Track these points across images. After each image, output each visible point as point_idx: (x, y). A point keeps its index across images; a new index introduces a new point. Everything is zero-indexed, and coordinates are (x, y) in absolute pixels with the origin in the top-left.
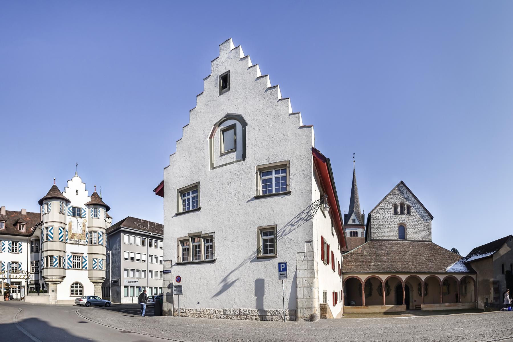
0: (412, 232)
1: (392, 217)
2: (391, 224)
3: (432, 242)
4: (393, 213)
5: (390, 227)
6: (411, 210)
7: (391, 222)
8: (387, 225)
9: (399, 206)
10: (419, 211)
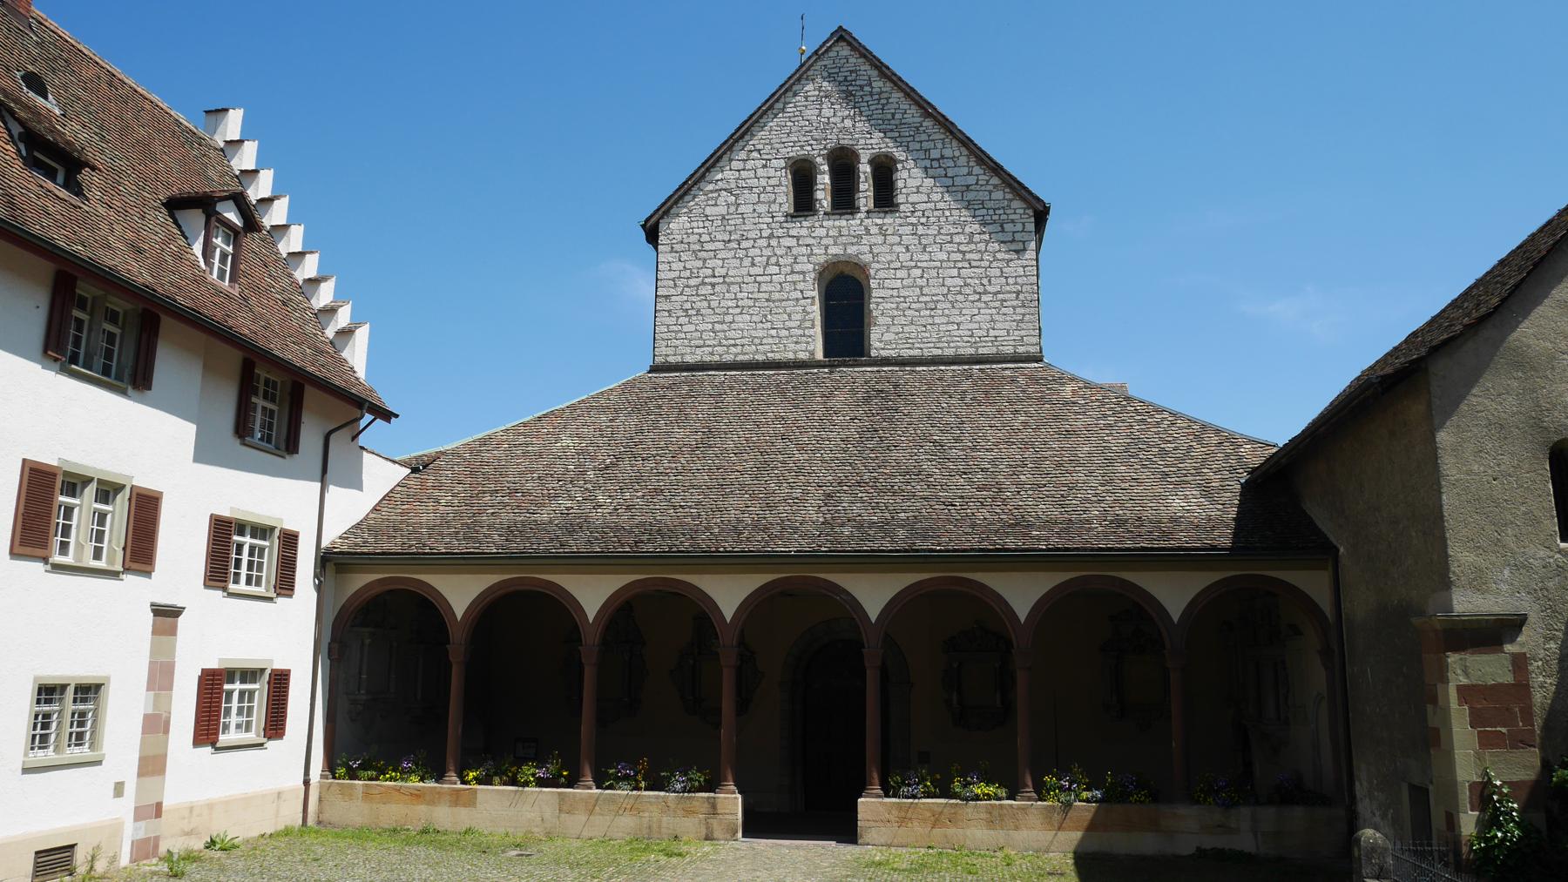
1: (780, 232)
2: (775, 269)
4: (788, 207)
6: (900, 184)
7: (773, 260)
9: (826, 168)
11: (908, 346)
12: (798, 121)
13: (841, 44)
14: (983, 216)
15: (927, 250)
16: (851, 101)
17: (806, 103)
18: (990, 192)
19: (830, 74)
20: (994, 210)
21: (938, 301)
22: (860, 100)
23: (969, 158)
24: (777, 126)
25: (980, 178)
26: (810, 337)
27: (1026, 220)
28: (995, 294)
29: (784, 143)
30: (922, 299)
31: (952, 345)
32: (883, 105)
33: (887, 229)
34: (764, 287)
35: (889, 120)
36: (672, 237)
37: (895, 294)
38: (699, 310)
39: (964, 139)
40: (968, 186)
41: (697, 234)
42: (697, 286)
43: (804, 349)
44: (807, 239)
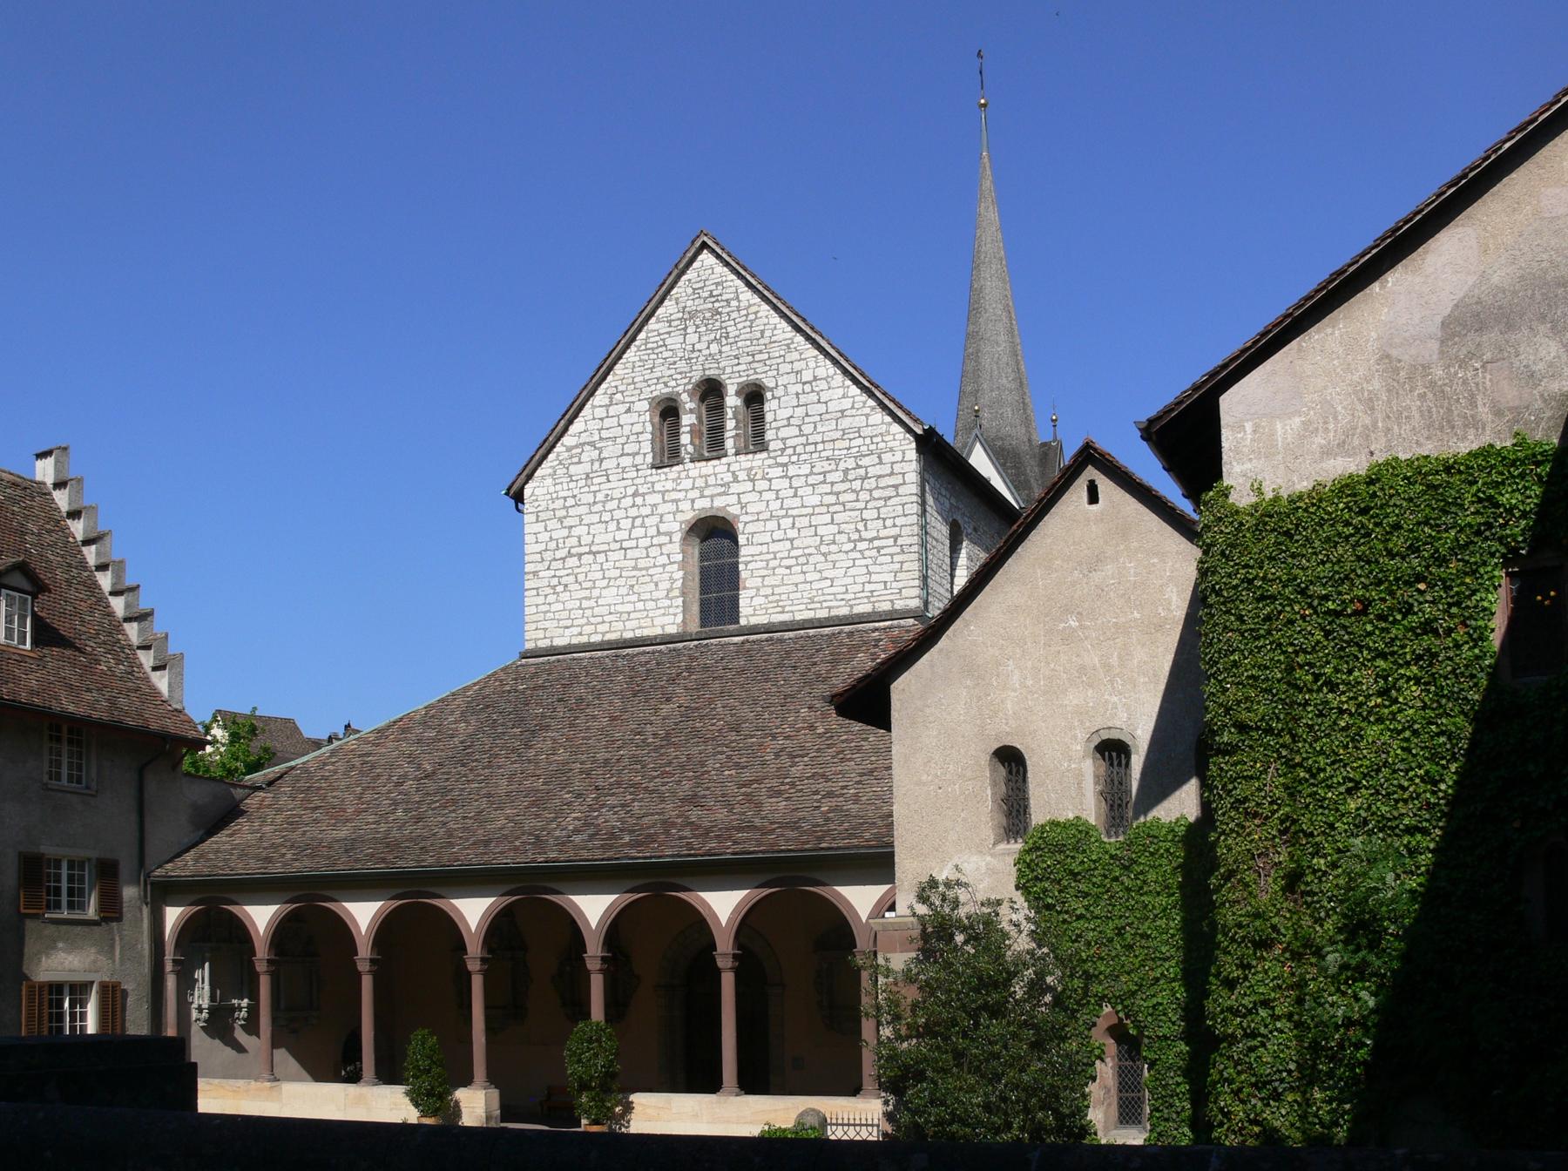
0: (773, 563)
4: (649, 459)
7: (638, 522)
8: (618, 546)
10: (822, 408)
11: (779, 609)
15: (799, 494)
16: (717, 320)
17: (671, 329)
18: (867, 416)
19: (694, 289)
24: (640, 360)
25: (857, 399)
26: (677, 607)
27: (906, 447)
28: (871, 540)
29: (646, 381)
30: (794, 553)
31: (825, 604)
32: (752, 321)
35: (758, 339)
38: (566, 586)
40: (842, 411)
42: (563, 559)
43: (671, 621)
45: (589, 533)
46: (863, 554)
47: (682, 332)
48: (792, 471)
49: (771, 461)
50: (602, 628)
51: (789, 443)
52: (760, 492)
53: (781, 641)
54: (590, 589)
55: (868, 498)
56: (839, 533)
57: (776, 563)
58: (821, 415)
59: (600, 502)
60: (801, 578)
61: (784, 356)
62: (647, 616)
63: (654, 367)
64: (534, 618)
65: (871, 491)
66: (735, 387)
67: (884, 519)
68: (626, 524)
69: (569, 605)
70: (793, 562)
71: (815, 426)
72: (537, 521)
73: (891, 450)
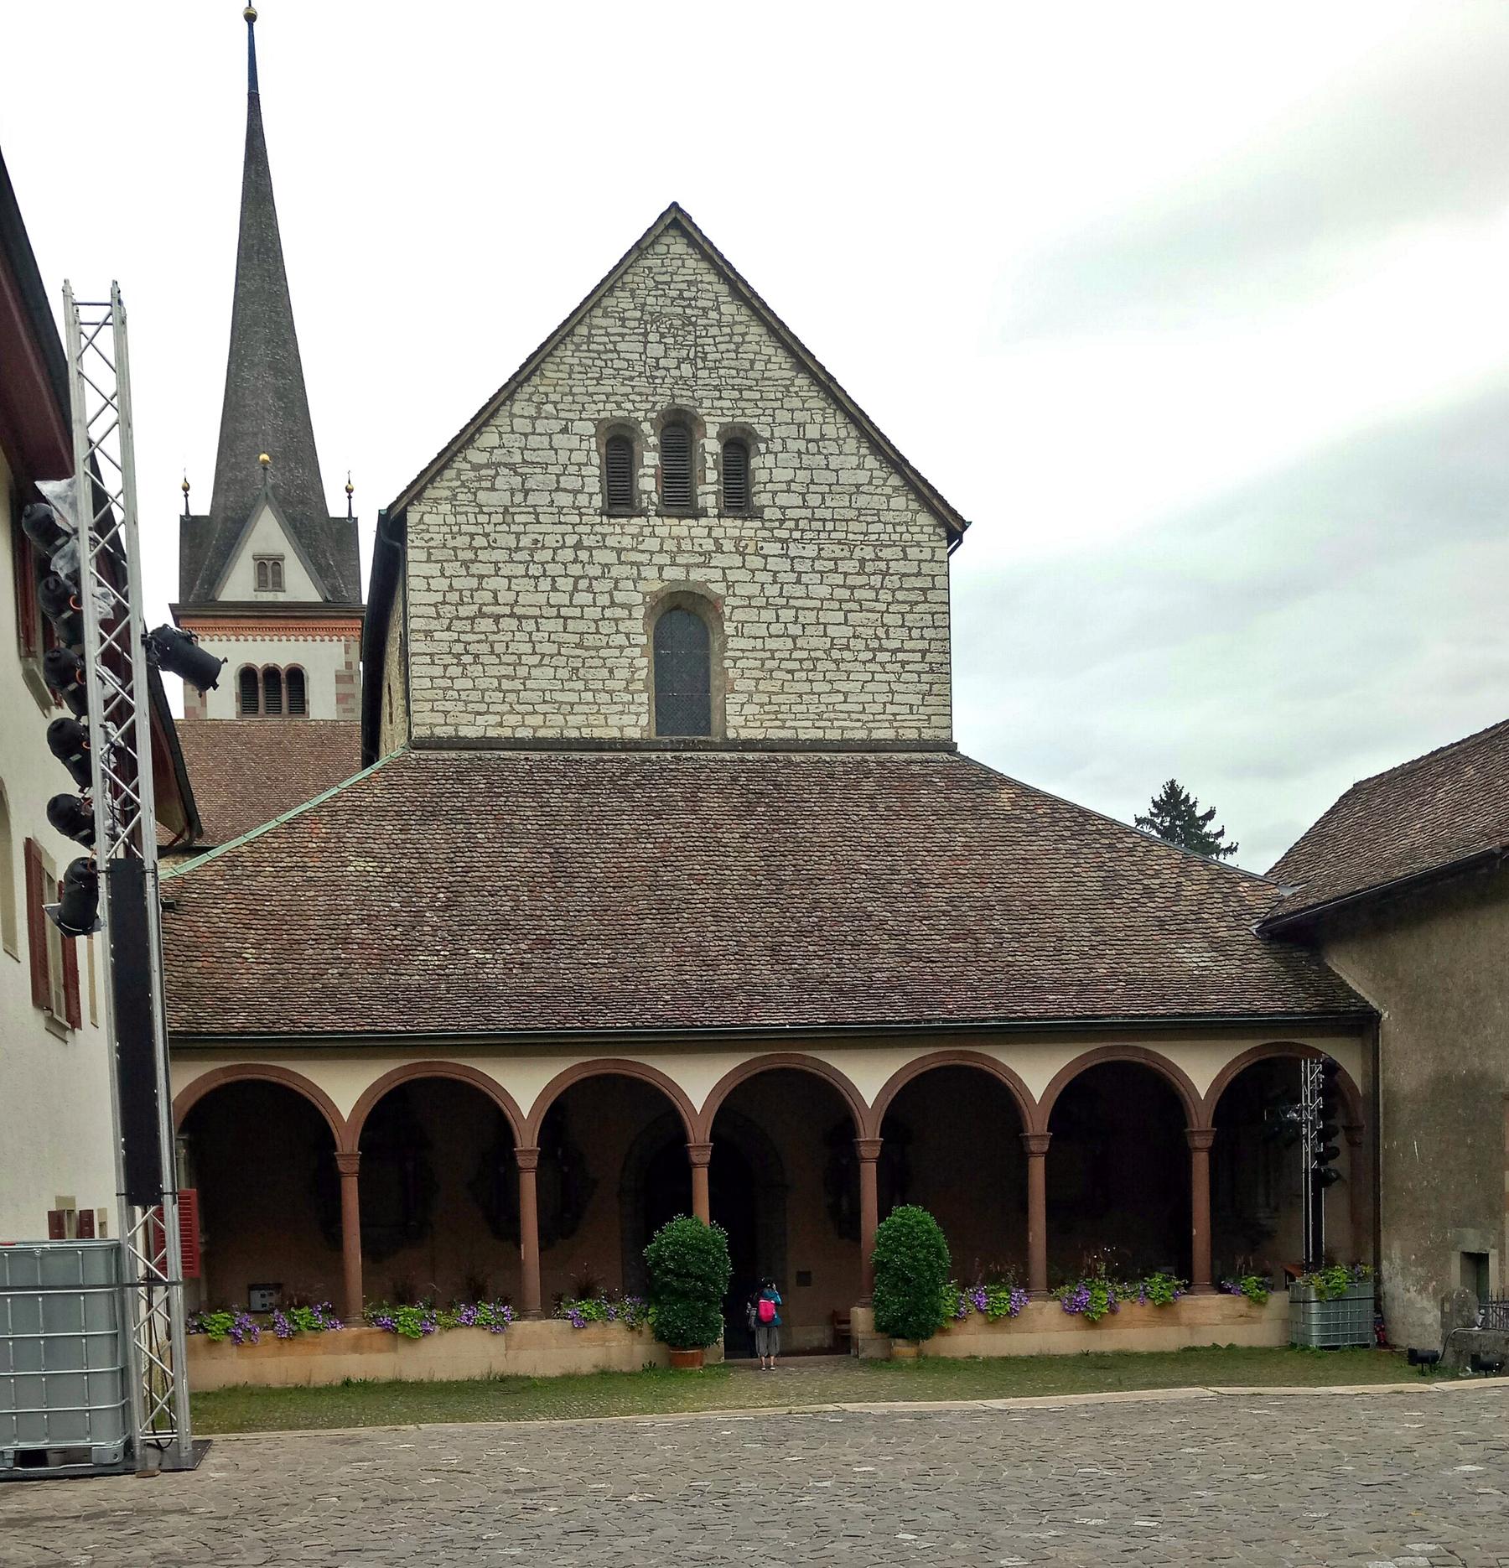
0: (769, 664)
2: (586, 598)
3: (950, 747)
4: (598, 501)
5: (581, 626)
6: (762, 476)
7: (583, 584)
11: (778, 723)
12: (612, 360)
13: (672, 232)
14: (879, 533)
18: (889, 497)
19: (658, 283)
20: (894, 525)
21: (818, 659)
22: (704, 333)
23: (859, 442)
24: (580, 364)
28: (894, 652)
29: (591, 395)
30: (797, 655)
31: (836, 724)
32: (738, 345)
33: (747, 545)
34: (571, 625)
35: (746, 371)
36: (430, 536)
37: (760, 646)
38: (476, 656)
39: (857, 414)
40: (858, 486)
41: (466, 534)
42: (472, 619)
44: (631, 553)
45: (509, 589)
46: (883, 667)
47: (641, 338)
48: (794, 550)
49: (766, 534)
50: (536, 720)
51: (790, 513)
52: (753, 571)
53: (789, 764)
54: (514, 665)
55: (890, 600)
56: (854, 637)
57: (775, 663)
58: (830, 485)
59: (524, 548)
60: (806, 687)
61: (782, 400)
62: (598, 712)
63: (601, 378)
64: (429, 695)
65: (894, 591)
66: (717, 428)
67: (910, 629)
68: (565, 584)
69: (482, 683)
70: (796, 665)
71: (823, 499)
72: (428, 561)
73: (918, 544)
